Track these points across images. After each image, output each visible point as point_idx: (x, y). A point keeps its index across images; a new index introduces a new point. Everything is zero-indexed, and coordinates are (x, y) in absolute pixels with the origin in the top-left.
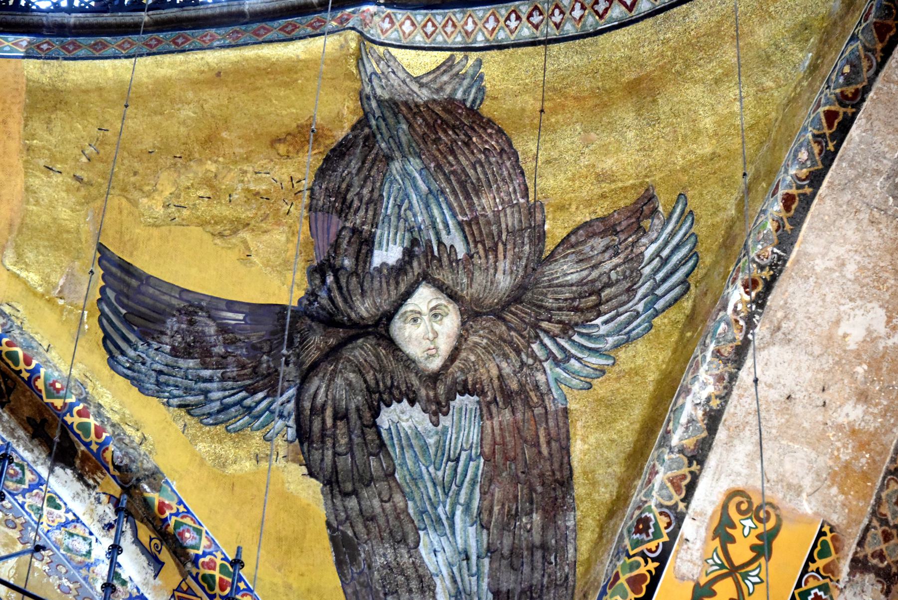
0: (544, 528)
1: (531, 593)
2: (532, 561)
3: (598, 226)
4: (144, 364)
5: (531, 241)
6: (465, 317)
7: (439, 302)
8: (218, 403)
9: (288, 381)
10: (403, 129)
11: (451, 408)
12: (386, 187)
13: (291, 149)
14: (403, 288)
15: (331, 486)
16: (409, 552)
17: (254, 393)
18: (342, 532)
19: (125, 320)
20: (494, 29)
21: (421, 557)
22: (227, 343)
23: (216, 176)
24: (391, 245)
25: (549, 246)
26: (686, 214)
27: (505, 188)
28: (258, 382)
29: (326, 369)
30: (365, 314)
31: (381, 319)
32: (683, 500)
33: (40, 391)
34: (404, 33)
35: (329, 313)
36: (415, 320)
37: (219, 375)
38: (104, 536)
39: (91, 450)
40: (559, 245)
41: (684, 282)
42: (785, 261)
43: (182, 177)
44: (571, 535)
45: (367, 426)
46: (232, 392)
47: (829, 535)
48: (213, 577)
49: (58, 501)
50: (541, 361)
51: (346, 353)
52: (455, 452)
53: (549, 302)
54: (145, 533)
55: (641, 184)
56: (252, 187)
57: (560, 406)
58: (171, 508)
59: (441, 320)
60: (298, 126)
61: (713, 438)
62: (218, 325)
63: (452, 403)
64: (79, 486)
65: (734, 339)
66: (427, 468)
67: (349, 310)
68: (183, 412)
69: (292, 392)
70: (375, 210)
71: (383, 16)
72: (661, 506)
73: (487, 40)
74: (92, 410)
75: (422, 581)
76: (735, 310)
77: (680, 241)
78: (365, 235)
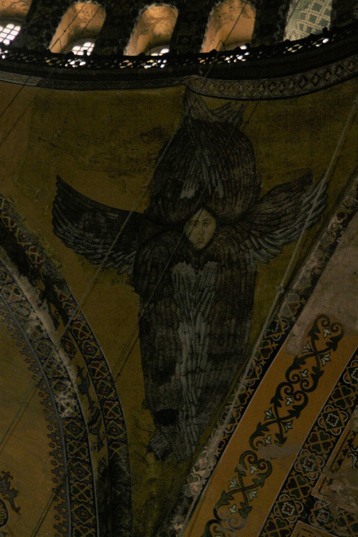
4: (69, 233)
16: (173, 331)
25: (261, 196)
30: (173, 220)
32: (295, 316)
33: (16, 238)
38: (38, 310)
39: (35, 268)
40: (265, 195)
48: (78, 331)
49: (20, 291)
53: (257, 221)
54: (53, 308)
58: (66, 298)
63: (206, 265)
64: (29, 285)
65: (330, 241)
69: (135, 252)
72: (284, 317)
73: (248, 96)
76: (332, 228)
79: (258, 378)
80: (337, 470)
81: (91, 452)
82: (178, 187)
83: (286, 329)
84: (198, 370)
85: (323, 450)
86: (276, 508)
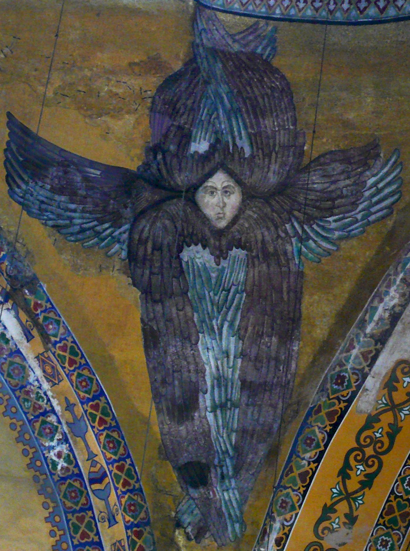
4: (32, 195)
5: (294, 154)
6: (245, 197)
7: (230, 184)
8: (79, 227)
9: (125, 219)
10: (219, 66)
11: (229, 255)
12: (204, 100)
14: (207, 170)
16: (191, 346)
17: (102, 223)
18: (150, 326)
20: (288, 6)
22: (88, 189)
24: (202, 140)
25: (306, 161)
26: (398, 163)
27: (281, 116)
28: (105, 216)
30: (180, 183)
32: (368, 366)
36: (212, 193)
37: (81, 208)
41: (390, 207)
43: (68, 77)
46: (88, 221)
50: (290, 237)
52: (228, 285)
53: (301, 199)
54: (24, 317)
56: (114, 90)
59: (229, 195)
63: (230, 253)
66: (209, 293)
69: (127, 226)
75: (197, 366)
77: (392, 180)
78: (186, 131)
79: (322, 448)
81: (99, 524)
83: (357, 384)
84: (229, 403)
85: (400, 523)
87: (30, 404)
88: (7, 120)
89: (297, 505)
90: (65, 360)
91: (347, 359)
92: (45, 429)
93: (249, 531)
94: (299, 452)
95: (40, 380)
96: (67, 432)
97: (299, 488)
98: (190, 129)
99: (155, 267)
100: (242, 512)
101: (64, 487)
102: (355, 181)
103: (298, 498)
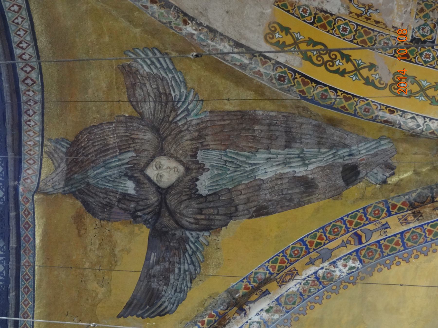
0: (261, 124)
1: (288, 132)
2: (274, 131)
3: (131, 92)
4: (172, 298)
5: (132, 122)
7: (154, 165)
8: (190, 266)
12: (99, 186)
13: (83, 228)
14: (146, 181)
15: (232, 216)
16: (265, 184)
17: (186, 250)
18: (253, 212)
19: (152, 306)
20: (34, 132)
21: (268, 178)
23: (91, 263)
24: (126, 186)
25: (135, 114)
27: (107, 133)
29: (179, 217)
30: (156, 199)
31: (159, 192)
32: (271, 61)
34: (32, 173)
35: (154, 215)
36: (161, 177)
39: (218, 320)
42: (176, 6)
44: (266, 113)
45: (206, 200)
46: (185, 259)
47: (278, 3)
48: (279, 266)
50: (187, 122)
51: (173, 208)
53: (161, 116)
55: (116, 70)
56: (97, 247)
57: (208, 114)
59: (162, 165)
60: (74, 224)
61: (245, 46)
62: (156, 264)
63: (200, 162)
65: (207, 32)
66: (228, 174)
67: (154, 206)
68: (194, 282)
69: (187, 233)
70: (110, 192)
71: (24, 182)
72: (273, 70)
73: (39, 136)
74: (200, 319)
76: (196, 30)
79: (327, 88)
80: (384, 24)
81: (389, 235)
82: (125, 197)
84: (301, 155)
86: (430, 65)
87: (312, 289)
88: (122, 318)
89: (366, 102)
90: (281, 266)
91: (267, 75)
92: (328, 277)
93: (385, 133)
94: (331, 103)
95: (295, 284)
96: (328, 263)
97: (355, 101)
98: (120, 194)
99: (214, 212)
100: (374, 140)
101: (366, 260)
102: (148, 81)
103: (361, 102)
